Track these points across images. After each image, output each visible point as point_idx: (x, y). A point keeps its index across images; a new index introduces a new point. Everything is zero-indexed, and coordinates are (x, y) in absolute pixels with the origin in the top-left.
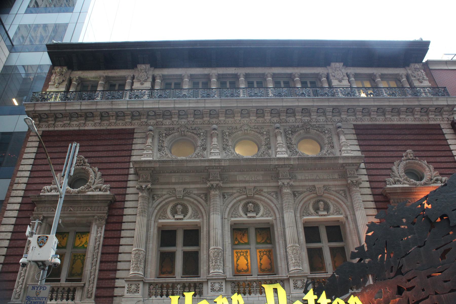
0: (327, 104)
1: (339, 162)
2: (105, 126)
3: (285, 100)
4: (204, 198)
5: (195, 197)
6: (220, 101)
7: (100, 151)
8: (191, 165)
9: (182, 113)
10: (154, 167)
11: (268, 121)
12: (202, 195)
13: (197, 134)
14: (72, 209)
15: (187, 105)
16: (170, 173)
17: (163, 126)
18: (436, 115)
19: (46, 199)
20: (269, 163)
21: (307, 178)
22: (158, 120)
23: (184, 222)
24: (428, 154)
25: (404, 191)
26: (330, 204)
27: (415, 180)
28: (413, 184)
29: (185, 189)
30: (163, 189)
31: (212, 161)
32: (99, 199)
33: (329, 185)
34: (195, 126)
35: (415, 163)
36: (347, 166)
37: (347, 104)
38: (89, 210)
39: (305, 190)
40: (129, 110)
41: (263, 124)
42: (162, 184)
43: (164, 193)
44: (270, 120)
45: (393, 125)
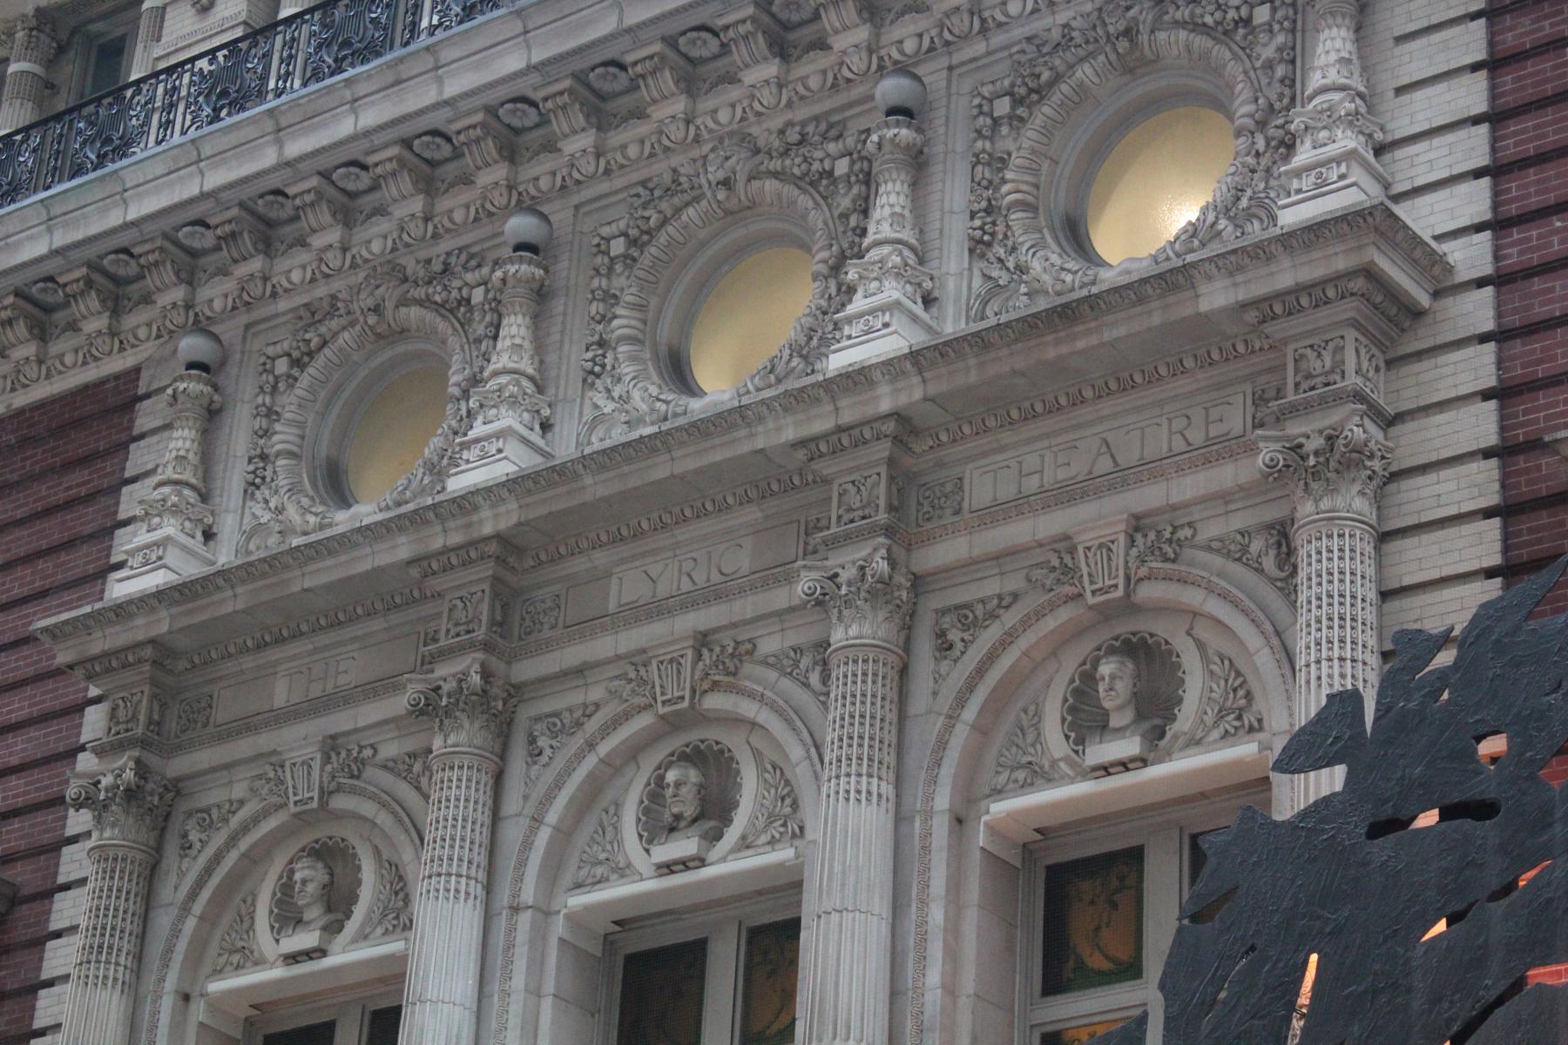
1: (1205, 306)
4: (1269, 563)
6: (518, 26)
8: (324, 579)
9: (346, 185)
10: (152, 642)
11: (857, 62)
12: (1256, 545)
13: (442, 308)
16: (261, 646)
17: (283, 305)
20: (745, 448)
21: (1032, 484)
26: (1191, 662)
29: (331, 745)
30: (227, 767)
31: (427, 522)
33: (1173, 508)
39: (1015, 583)
40: (74, 255)
41: (841, 99)
42: (226, 734)
43: (239, 791)
44: (188, 306)
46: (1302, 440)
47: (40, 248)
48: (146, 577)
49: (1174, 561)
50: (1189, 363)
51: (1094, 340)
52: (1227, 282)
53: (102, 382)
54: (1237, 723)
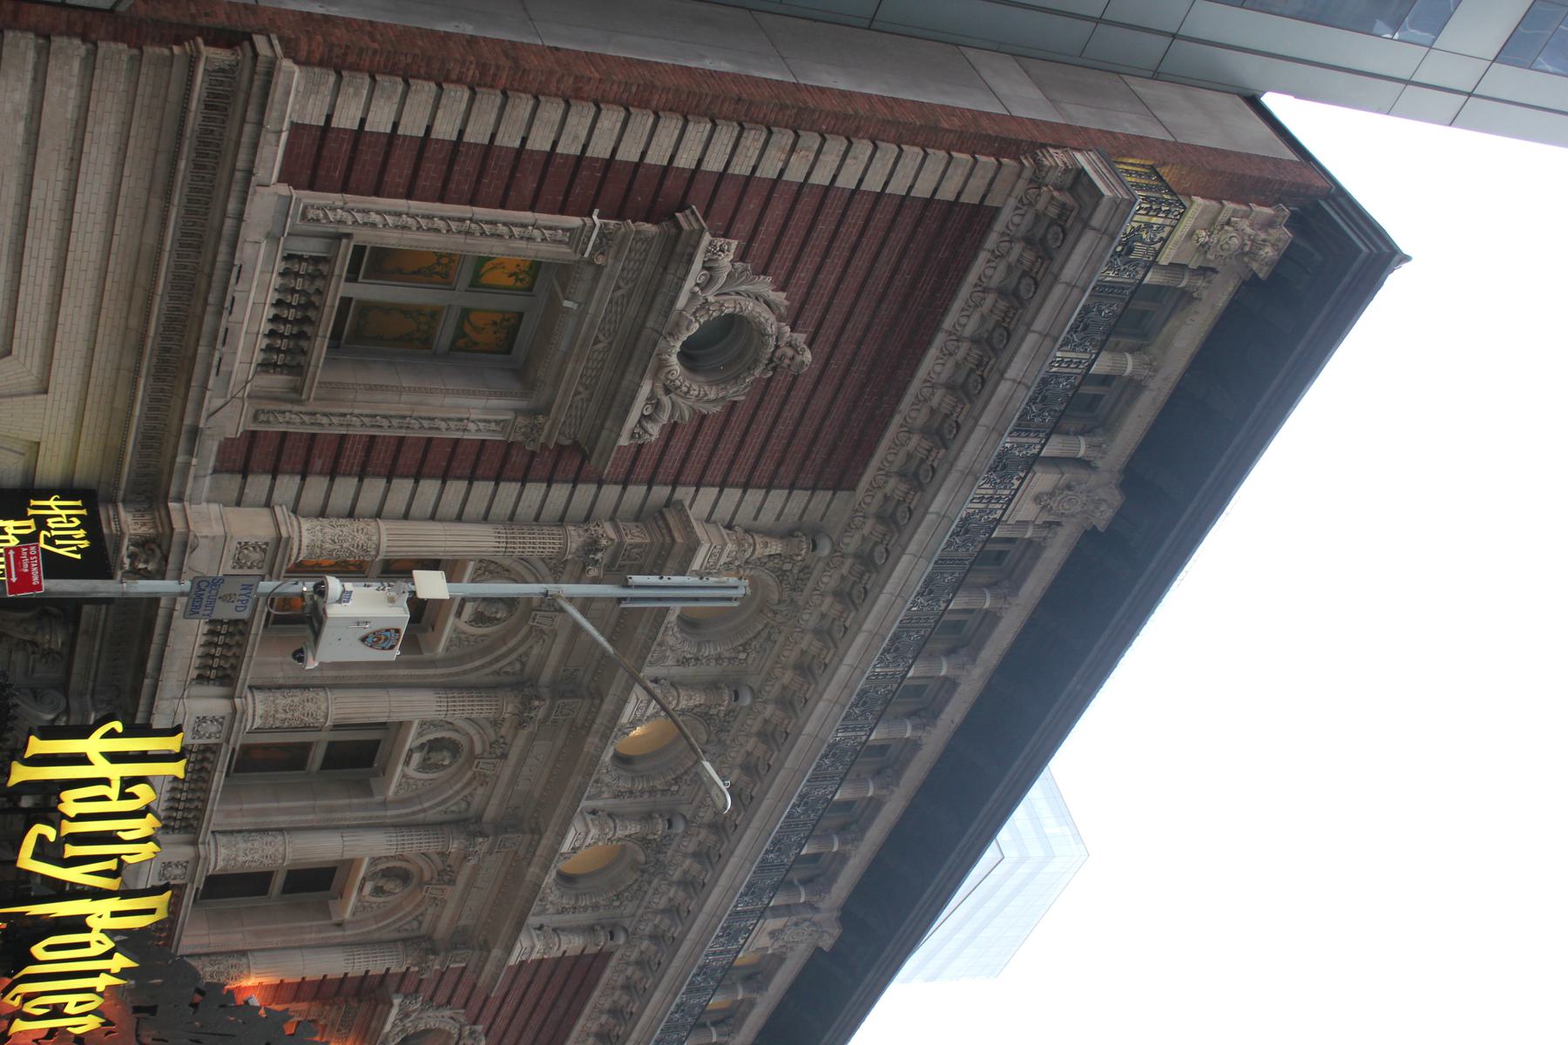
0: (692, 935)
2: (909, 410)
3: (747, 865)
5: (522, 650)
7: (889, 230)
9: (831, 635)
14: (600, 346)
15: (849, 659)
18: (909, 456)
19: (669, 277)
22: (849, 562)
23: (396, 765)
32: (605, 433)
34: (781, 639)
37: (671, 971)
38: (577, 393)
45: (578, 1015)
47: (934, 508)
53: (866, 465)
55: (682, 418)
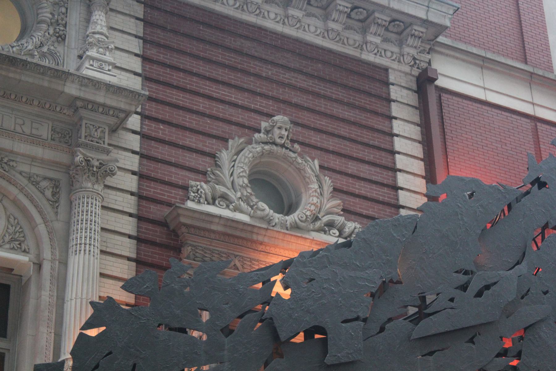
18: (385, 40)
24: (331, 143)
25: (229, 231)
27: (271, 207)
28: (262, 219)
33: (12, 152)
35: (285, 158)
36: (85, 108)
46: (91, 159)
48: (96, 72)
49: (7, 172)
50: (36, 103)
51: (17, 77)
52: (78, 87)
54: (19, 246)
55: (339, 205)
